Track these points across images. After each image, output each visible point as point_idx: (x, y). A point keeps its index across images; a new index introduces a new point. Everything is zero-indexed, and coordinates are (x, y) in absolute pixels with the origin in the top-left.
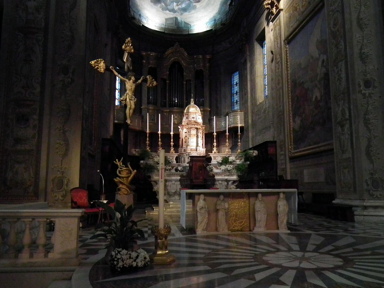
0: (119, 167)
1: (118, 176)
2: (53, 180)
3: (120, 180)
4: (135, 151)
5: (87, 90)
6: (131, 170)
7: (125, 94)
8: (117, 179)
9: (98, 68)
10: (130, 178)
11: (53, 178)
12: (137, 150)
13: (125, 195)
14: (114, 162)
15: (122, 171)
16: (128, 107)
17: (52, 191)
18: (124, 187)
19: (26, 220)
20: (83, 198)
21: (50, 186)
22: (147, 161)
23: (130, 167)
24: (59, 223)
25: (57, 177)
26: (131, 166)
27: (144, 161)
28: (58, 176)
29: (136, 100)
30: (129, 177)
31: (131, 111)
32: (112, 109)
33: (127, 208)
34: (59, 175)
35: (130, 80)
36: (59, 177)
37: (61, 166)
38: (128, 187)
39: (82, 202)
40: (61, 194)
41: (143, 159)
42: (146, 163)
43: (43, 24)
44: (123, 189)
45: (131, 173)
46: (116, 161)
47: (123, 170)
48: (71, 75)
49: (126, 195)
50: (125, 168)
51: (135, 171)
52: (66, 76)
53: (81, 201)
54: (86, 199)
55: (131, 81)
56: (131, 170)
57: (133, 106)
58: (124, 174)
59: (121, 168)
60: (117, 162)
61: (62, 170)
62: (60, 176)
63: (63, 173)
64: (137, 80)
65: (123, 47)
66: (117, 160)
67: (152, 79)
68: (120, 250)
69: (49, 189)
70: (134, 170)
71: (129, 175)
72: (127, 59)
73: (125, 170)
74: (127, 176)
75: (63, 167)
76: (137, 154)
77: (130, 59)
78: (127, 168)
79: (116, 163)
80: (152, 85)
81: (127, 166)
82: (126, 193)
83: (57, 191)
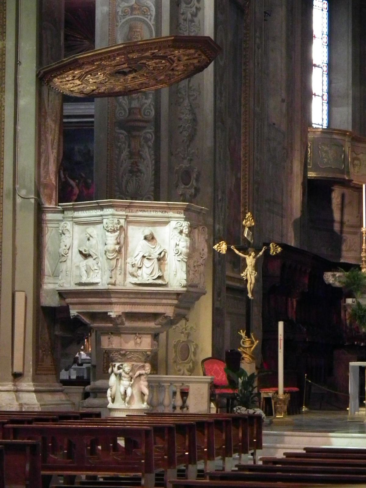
0: (243, 338)
1: (241, 346)
2: (175, 346)
3: (244, 350)
4: (334, 276)
5: (220, 198)
6: (254, 340)
7: (246, 270)
8: (240, 349)
9: (220, 251)
10: (252, 349)
11: (175, 343)
12: (338, 274)
13: (248, 364)
14: (239, 333)
15: (245, 341)
16: (249, 282)
17: (175, 362)
18: (247, 356)
19: (166, 384)
20: (220, 373)
21: (172, 355)
22: (361, 301)
23: (253, 338)
24: (193, 389)
25: (181, 341)
26: (254, 337)
27: (354, 300)
28: (182, 340)
29: (256, 274)
30: (251, 347)
31: (252, 286)
32: (297, 146)
33: (250, 376)
34: (183, 338)
35: (250, 255)
36: (183, 342)
37: (185, 326)
38: (250, 356)
39: (219, 379)
40: (187, 366)
41: (350, 296)
42: (359, 304)
43: (153, 113)
44: (247, 357)
45: (252, 343)
46: (240, 332)
47: (246, 341)
48: (194, 184)
49: (248, 363)
50: (247, 339)
51: (257, 342)
52: (188, 187)
53: (217, 379)
54: (224, 376)
55: (251, 257)
56: (254, 340)
57: (253, 281)
58: (247, 345)
59: (244, 339)
60: (242, 333)
61: (187, 331)
62: (186, 340)
63: (188, 335)
64: (257, 253)
65: (244, 222)
66: (241, 331)
67: (276, 246)
68: (240, 407)
69: (171, 361)
70: (256, 341)
71: (252, 345)
72: (248, 235)
73: (248, 340)
74: (249, 346)
75: (188, 326)
76: (337, 284)
77: (251, 233)
78: (249, 339)
79: (241, 334)
80: (276, 252)
81: (249, 337)
82: (249, 362)
83: (181, 362)
